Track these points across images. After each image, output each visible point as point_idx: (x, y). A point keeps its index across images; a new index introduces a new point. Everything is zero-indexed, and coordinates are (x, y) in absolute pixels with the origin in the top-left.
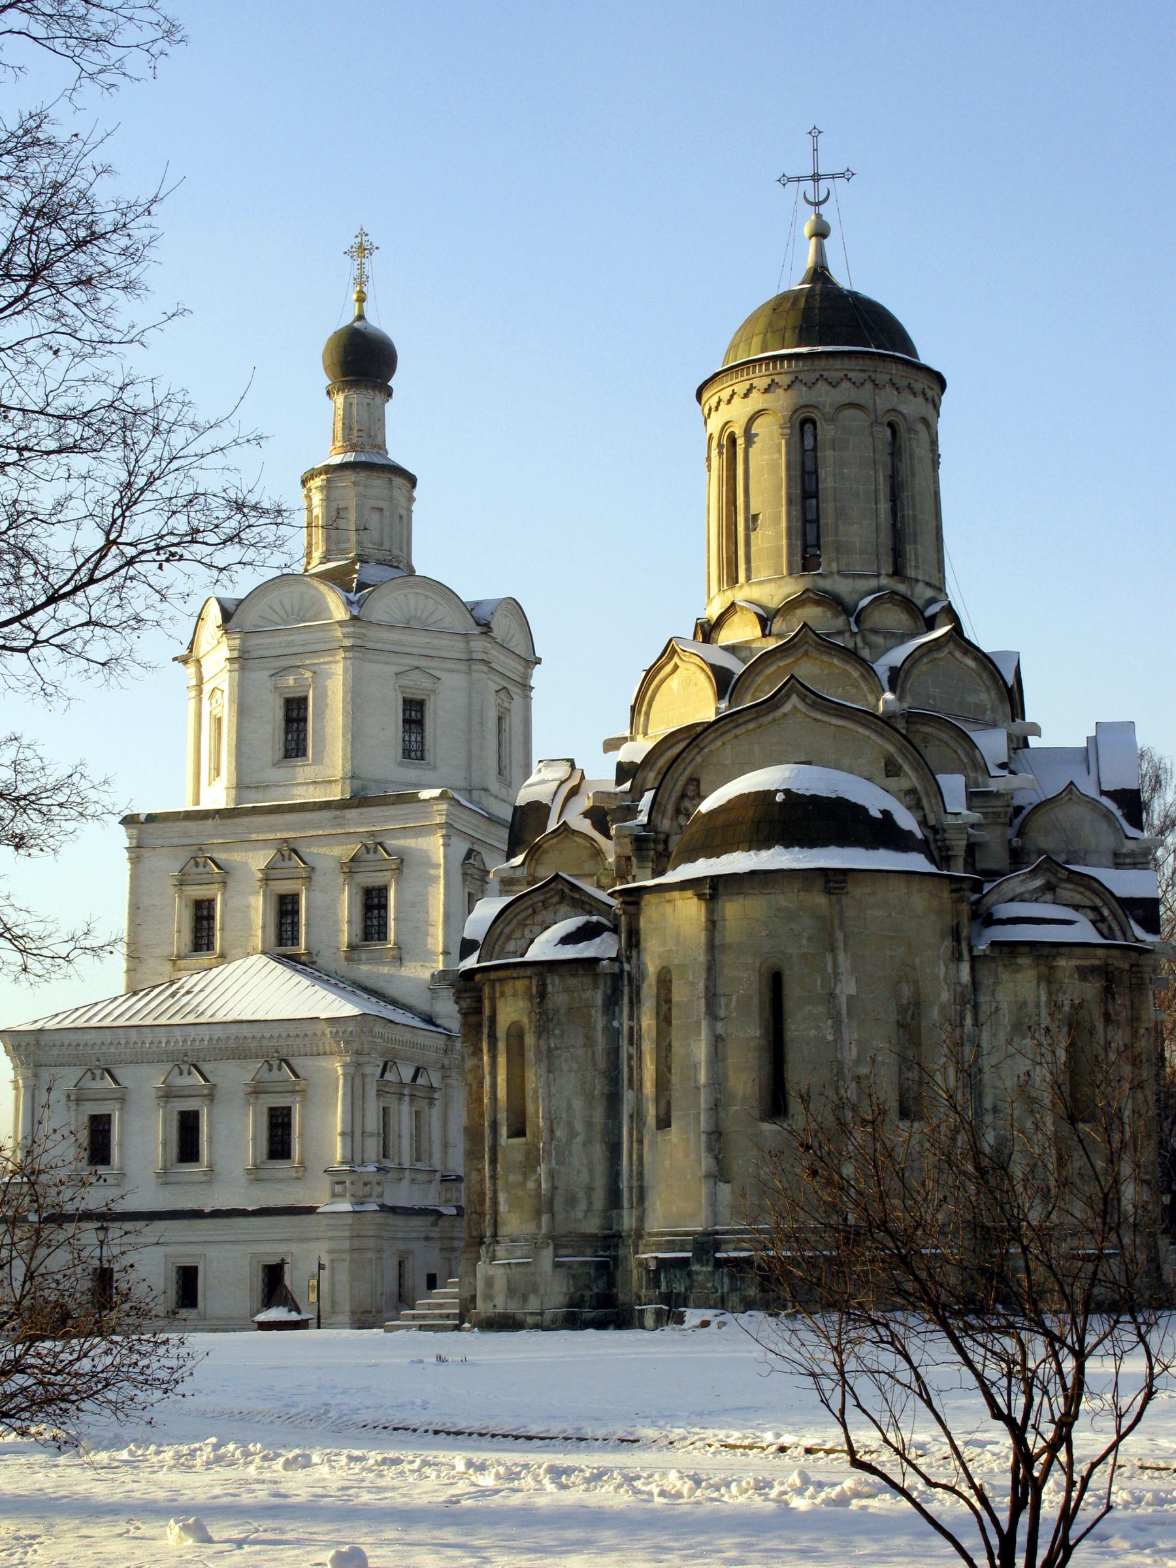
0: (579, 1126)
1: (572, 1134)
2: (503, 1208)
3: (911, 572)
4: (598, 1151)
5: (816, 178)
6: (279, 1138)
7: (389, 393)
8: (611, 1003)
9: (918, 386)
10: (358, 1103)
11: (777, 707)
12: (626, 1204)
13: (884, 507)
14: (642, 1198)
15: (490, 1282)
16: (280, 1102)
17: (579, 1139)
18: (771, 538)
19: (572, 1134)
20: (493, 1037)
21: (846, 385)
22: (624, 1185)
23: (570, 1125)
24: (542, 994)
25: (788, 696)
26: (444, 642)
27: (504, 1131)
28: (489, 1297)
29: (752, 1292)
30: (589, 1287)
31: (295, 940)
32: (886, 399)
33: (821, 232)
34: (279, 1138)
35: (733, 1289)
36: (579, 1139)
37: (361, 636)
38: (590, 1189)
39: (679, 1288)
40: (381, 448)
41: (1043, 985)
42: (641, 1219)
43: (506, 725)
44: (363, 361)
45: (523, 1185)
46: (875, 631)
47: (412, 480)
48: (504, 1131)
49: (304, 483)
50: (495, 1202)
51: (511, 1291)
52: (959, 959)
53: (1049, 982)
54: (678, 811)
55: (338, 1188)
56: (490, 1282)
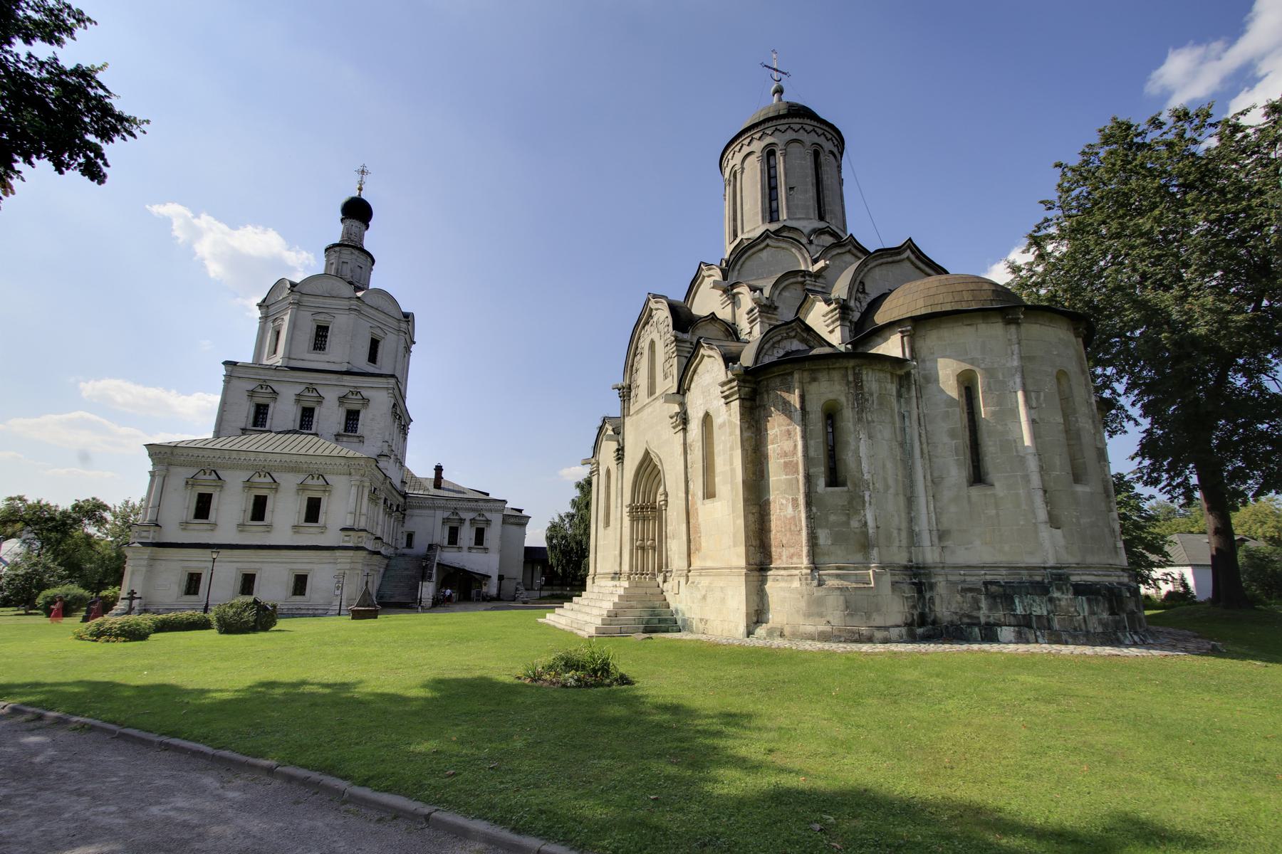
0: (891, 482)
1: (887, 488)
4: (902, 501)
17: (892, 491)
19: (887, 488)
23: (885, 479)
26: (390, 320)
29: (1105, 616)
35: (1092, 613)
36: (892, 491)
44: (357, 211)
45: (848, 523)
47: (373, 261)
48: (821, 483)
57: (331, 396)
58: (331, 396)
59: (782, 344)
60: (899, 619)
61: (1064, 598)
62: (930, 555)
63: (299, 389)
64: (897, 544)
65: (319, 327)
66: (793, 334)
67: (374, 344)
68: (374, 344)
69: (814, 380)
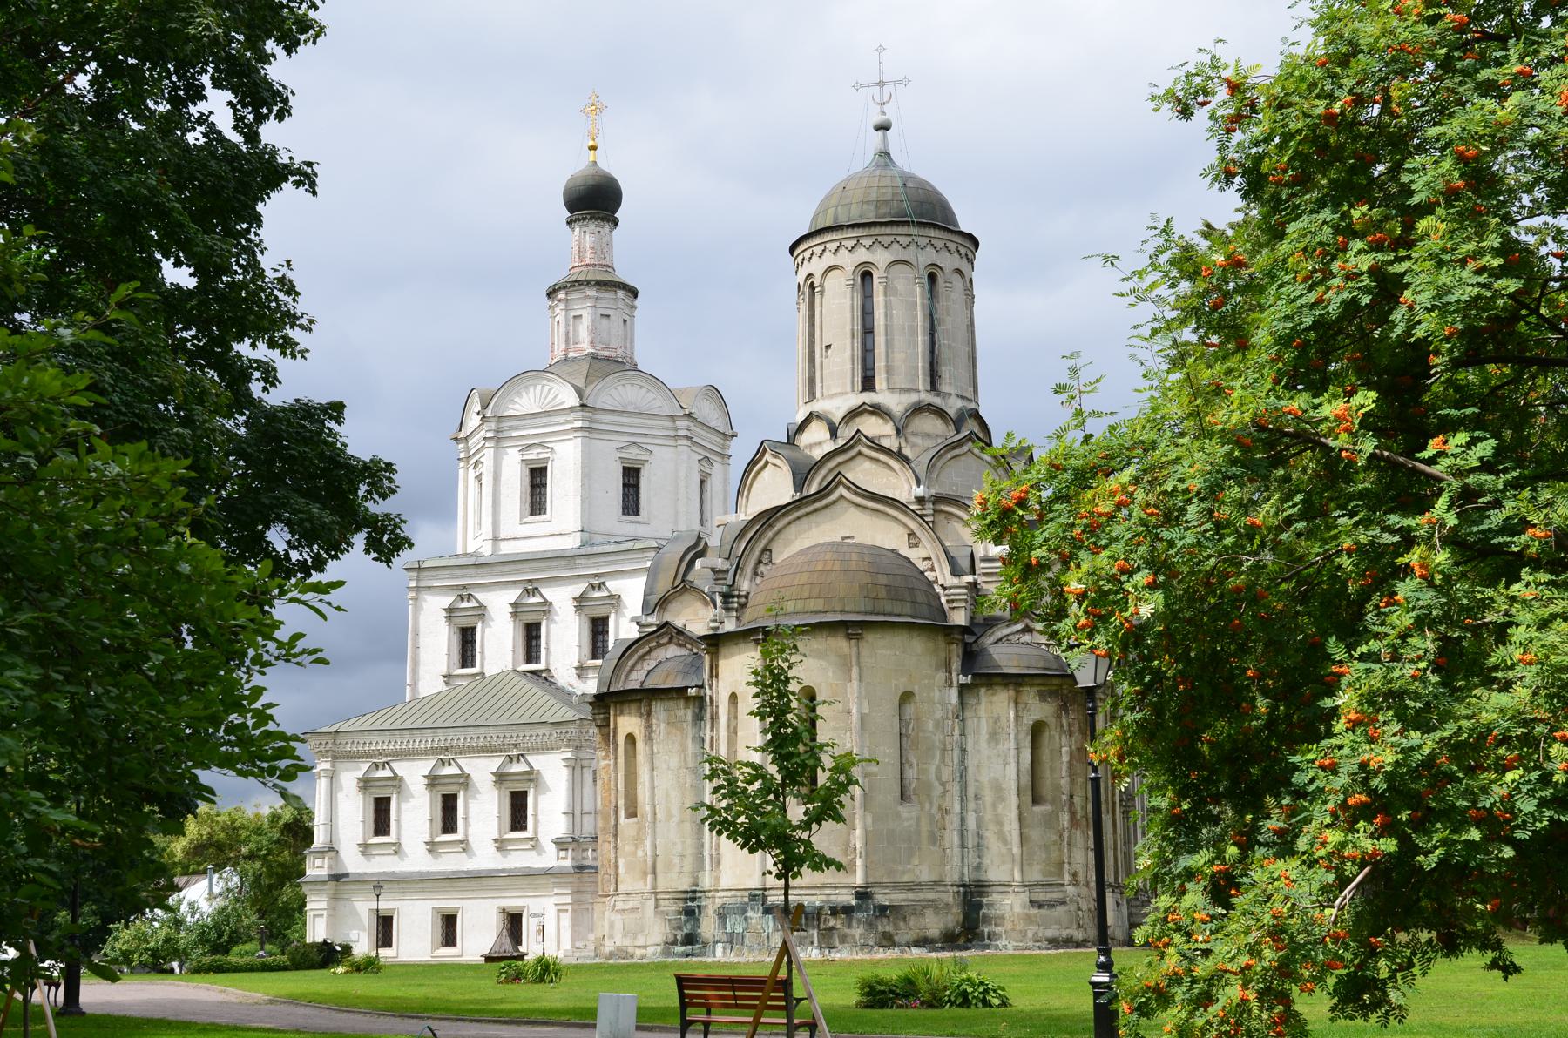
0: (675, 811)
1: (669, 816)
2: (621, 870)
3: (945, 387)
5: (881, 84)
6: (518, 813)
7: (616, 223)
8: (698, 718)
9: (952, 247)
10: (577, 790)
11: (829, 494)
12: (708, 868)
13: (922, 339)
14: (718, 863)
15: (612, 926)
16: (519, 787)
18: (840, 363)
20: (615, 741)
21: (895, 246)
22: (706, 853)
24: (649, 714)
25: (836, 487)
27: (622, 813)
28: (611, 937)
30: (680, 928)
31: (537, 660)
32: (927, 257)
33: (883, 127)
34: (518, 813)
36: (675, 820)
37: (590, 420)
38: (682, 856)
39: (739, 929)
40: (609, 267)
41: (1012, 705)
42: (717, 879)
43: (707, 486)
45: (635, 854)
46: (914, 434)
47: (634, 293)
48: (622, 813)
49: (550, 295)
50: (616, 867)
51: (626, 931)
52: (951, 686)
53: (1016, 703)
54: (756, 574)
55: (562, 854)
56: (612, 926)
57: (561, 597)
58: (561, 597)
59: (653, 654)
60: (659, 939)
61: (755, 915)
62: (706, 882)
63: (513, 594)
64: (677, 869)
65: (533, 471)
66: (665, 640)
67: (631, 476)
68: (631, 476)
69: (622, 713)
